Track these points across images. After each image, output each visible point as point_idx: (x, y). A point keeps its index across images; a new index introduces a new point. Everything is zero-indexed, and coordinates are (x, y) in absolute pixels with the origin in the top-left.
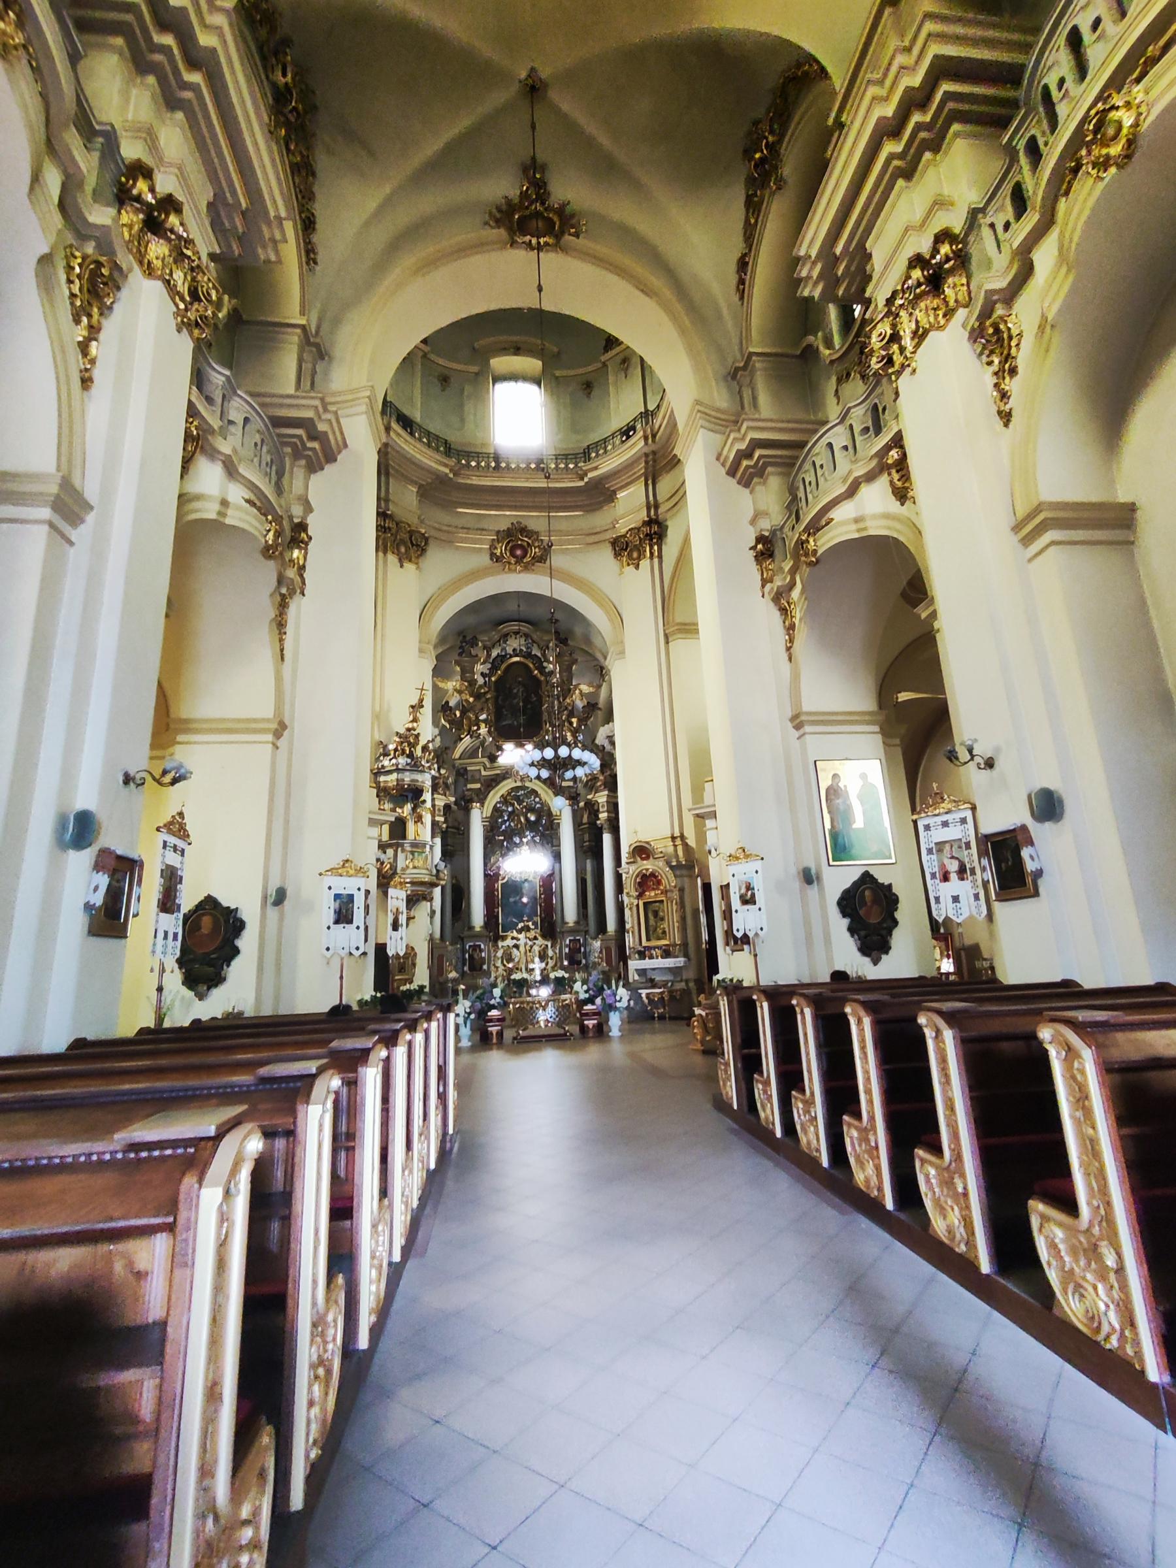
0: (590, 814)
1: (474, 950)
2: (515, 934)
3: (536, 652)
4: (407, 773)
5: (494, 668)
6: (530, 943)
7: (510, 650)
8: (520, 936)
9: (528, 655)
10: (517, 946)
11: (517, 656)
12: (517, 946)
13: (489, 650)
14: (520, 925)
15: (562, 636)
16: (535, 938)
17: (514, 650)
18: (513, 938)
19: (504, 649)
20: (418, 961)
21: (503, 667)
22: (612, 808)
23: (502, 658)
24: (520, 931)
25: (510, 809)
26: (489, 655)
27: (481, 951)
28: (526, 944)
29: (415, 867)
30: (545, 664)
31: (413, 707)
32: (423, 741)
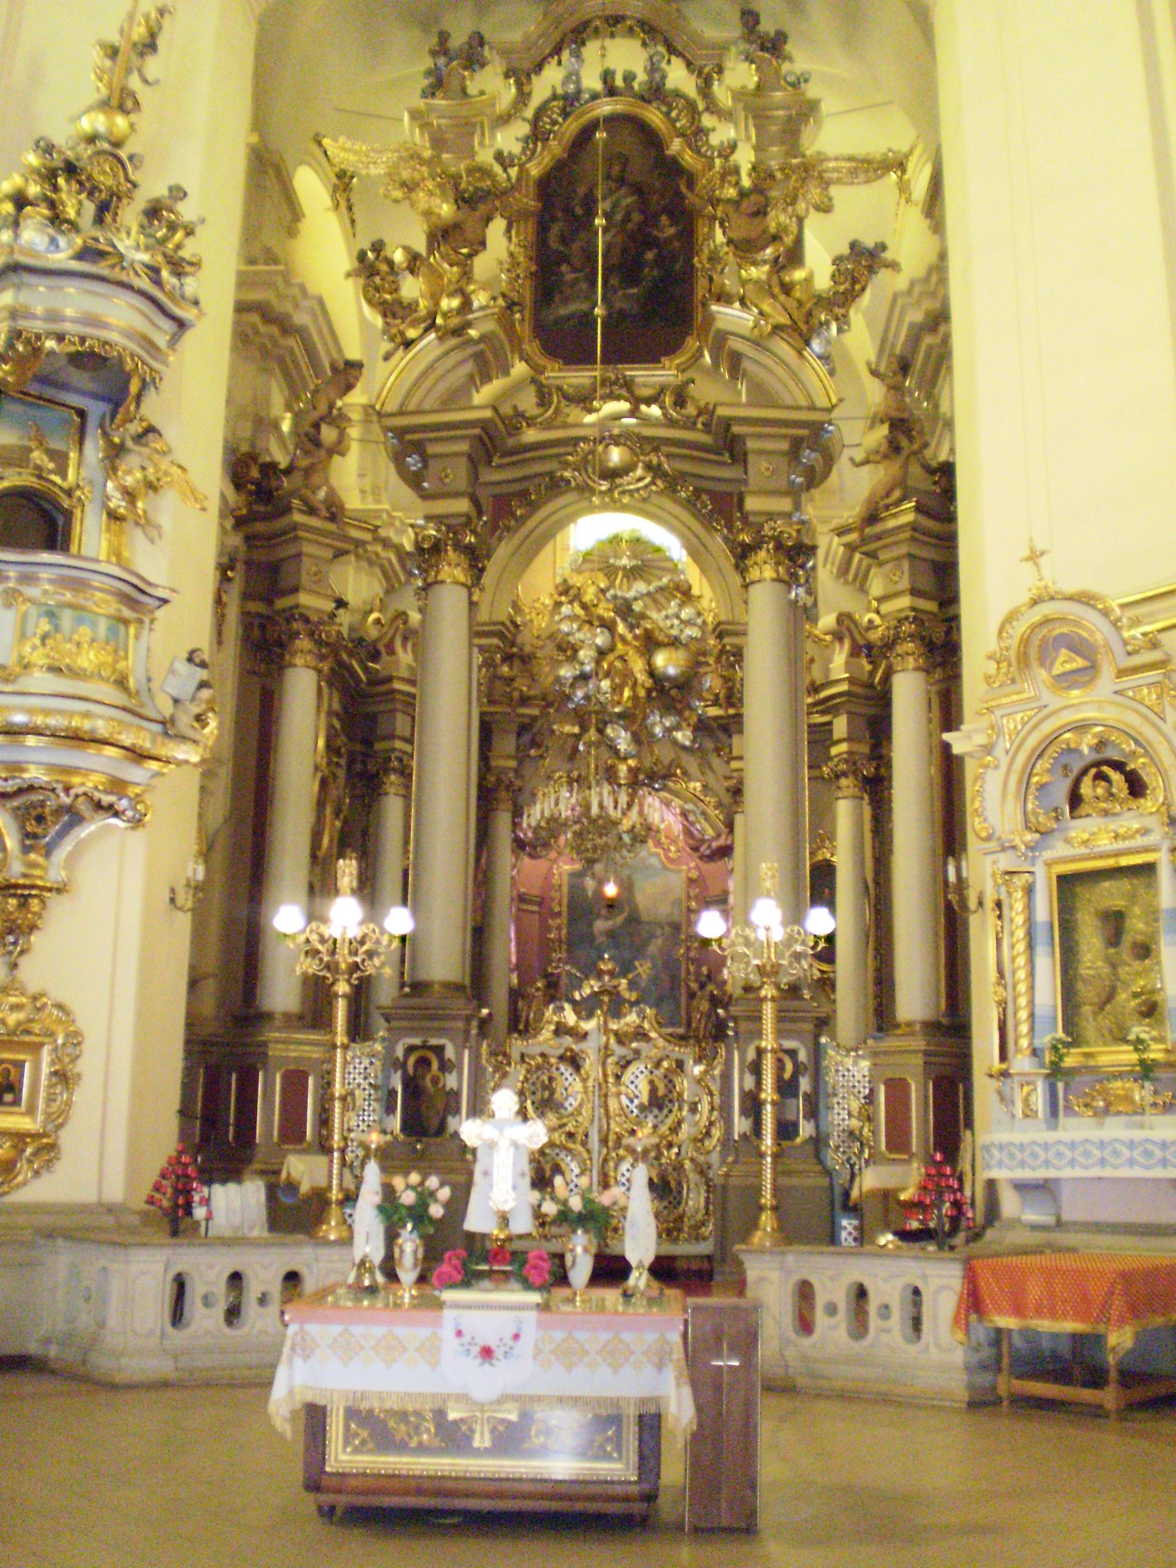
0: (855, 652)
1: (423, 1062)
2: (570, 1017)
3: (678, 76)
4: (71, 288)
5: (537, 135)
6: (620, 1051)
7: (592, 81)
8: (589, 1026)
9: (656, 92)
10: (574, 1062)
11: (611, 91)
12: (574, 1062)
13: (521, 75)
14: (591, 986)
15: (767, 26)
16: (640, 1034)
17: (607, 77)
18: (561, 1030)
19: (573, 76)
20: (82, 1066)
21: (571, 127)
22: (926, 582)
23: (569, 101)
24: (585, 1009)
25: (601, 639)
26: (523, 96)
27: (445, 1066)
28: (606, 1051)
29: (55, 669)
30: (707, 121)
31: (113, 52)
32: (152, 187)
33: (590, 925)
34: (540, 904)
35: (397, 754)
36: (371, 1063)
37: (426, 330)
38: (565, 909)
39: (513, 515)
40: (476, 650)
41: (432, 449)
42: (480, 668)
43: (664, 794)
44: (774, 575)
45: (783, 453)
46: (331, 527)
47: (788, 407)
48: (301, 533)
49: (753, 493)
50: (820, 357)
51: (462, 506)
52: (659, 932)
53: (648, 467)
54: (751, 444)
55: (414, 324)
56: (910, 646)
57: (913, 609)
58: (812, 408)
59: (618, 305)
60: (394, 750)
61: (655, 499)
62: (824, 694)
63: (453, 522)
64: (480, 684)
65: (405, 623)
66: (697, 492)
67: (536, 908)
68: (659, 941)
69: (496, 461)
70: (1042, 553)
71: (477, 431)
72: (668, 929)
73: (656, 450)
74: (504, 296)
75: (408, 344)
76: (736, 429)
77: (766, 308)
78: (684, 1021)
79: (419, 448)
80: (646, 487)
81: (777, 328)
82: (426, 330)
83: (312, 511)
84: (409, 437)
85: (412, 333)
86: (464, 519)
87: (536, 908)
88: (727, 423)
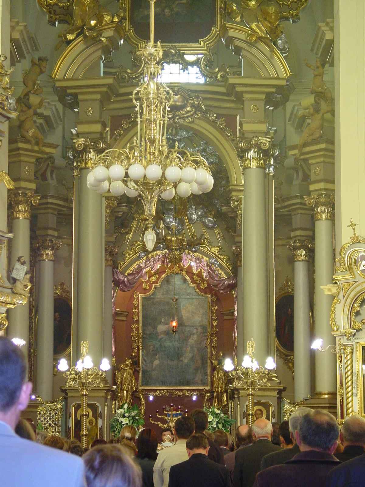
33: (155, 328)
34: (126, 316)
35: (50, 237)
36: (56, 414)
37: (78, 36)
38: (141, 319)
39: (122, 127)
40: (104, 199)
41: (80, 97)
42: (106, 208)
43: (196, 254)
44: (257, 165)
45: (262, 100)
46: (36, 148)
47: (265, 78)
48: (21, 152)
49: (247, 122)
50: (281, 50)
51: (97, 128)
52: (195, 331)
53: (193, 106)
54: (245, 96)
55: (71, 32)
56: (323, 208)
57: (325, 189)
58: (278, 78)
59: (176, 9)
60: (48, 235)
61: (197, 121)
62: (287, 203)
63: (92, 136)
64: (106, 217)
65: (53, 163)
66: (218, 117)
67: (124, 318)
68: (195, 336)
69: (113, 99)
70: (355, 225)
71: (105, 89)
72: (200, 330)
73: (197, 97)
74: (118, 16)
75: (69, 42)
76: (238, 89)
77: (254, 26)
78: (209, 383)
79: (75, 96)
80: (192, 115)
81: (260, 38)
82: (78, 36)
83: (28, 142)
84: (69, 91)
85: (70, 37)
86: (98, 136)
87: (124, 318)
88: (234, 86)
